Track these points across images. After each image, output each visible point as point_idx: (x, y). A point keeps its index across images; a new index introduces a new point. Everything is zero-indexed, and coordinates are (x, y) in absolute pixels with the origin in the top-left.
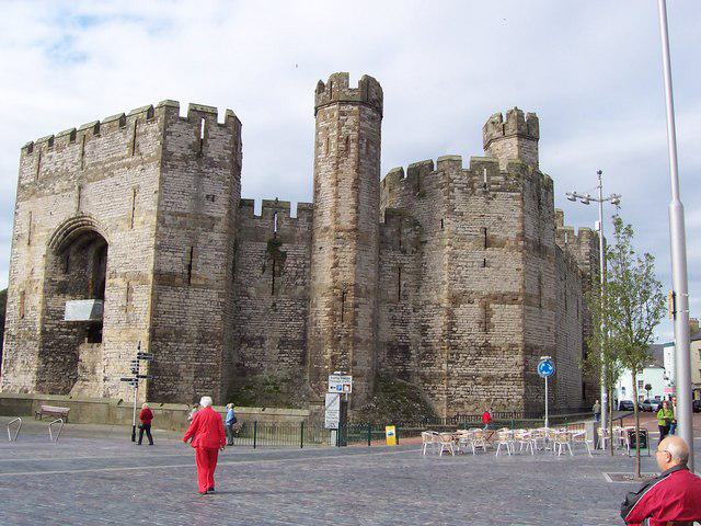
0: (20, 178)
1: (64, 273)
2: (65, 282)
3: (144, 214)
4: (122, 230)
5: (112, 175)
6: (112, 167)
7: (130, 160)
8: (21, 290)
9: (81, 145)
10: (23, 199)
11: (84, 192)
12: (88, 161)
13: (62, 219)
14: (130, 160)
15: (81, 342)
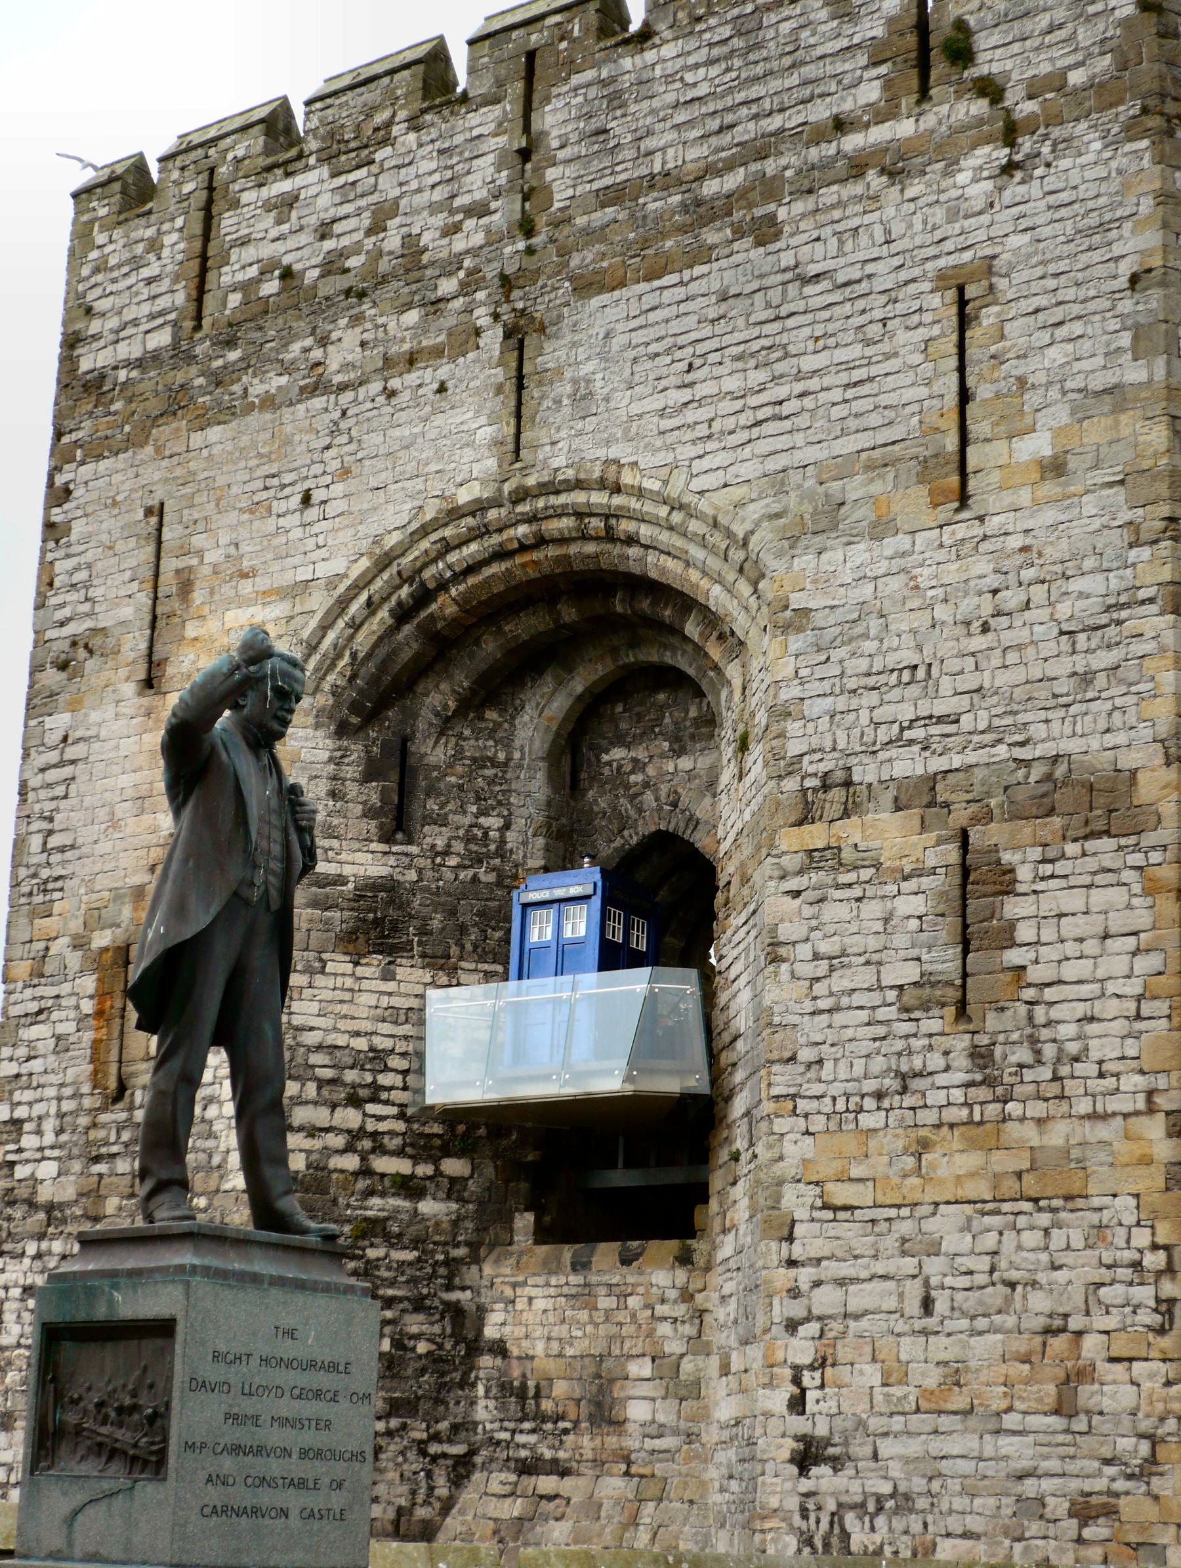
0: (72, 342)
1: (387, 838)
2: (389, 886)
3: (1061, 415)
4: (880, 529)
5: (766, 232)
6: (770, 188)
7: (905, 128)
8: (102, 939)
9: (510, 106)
10: (96, 451)
11: (549, 355)
12: (562, 183)
13: (391, 519)
14: (905, 128)
15: (487, 1233)
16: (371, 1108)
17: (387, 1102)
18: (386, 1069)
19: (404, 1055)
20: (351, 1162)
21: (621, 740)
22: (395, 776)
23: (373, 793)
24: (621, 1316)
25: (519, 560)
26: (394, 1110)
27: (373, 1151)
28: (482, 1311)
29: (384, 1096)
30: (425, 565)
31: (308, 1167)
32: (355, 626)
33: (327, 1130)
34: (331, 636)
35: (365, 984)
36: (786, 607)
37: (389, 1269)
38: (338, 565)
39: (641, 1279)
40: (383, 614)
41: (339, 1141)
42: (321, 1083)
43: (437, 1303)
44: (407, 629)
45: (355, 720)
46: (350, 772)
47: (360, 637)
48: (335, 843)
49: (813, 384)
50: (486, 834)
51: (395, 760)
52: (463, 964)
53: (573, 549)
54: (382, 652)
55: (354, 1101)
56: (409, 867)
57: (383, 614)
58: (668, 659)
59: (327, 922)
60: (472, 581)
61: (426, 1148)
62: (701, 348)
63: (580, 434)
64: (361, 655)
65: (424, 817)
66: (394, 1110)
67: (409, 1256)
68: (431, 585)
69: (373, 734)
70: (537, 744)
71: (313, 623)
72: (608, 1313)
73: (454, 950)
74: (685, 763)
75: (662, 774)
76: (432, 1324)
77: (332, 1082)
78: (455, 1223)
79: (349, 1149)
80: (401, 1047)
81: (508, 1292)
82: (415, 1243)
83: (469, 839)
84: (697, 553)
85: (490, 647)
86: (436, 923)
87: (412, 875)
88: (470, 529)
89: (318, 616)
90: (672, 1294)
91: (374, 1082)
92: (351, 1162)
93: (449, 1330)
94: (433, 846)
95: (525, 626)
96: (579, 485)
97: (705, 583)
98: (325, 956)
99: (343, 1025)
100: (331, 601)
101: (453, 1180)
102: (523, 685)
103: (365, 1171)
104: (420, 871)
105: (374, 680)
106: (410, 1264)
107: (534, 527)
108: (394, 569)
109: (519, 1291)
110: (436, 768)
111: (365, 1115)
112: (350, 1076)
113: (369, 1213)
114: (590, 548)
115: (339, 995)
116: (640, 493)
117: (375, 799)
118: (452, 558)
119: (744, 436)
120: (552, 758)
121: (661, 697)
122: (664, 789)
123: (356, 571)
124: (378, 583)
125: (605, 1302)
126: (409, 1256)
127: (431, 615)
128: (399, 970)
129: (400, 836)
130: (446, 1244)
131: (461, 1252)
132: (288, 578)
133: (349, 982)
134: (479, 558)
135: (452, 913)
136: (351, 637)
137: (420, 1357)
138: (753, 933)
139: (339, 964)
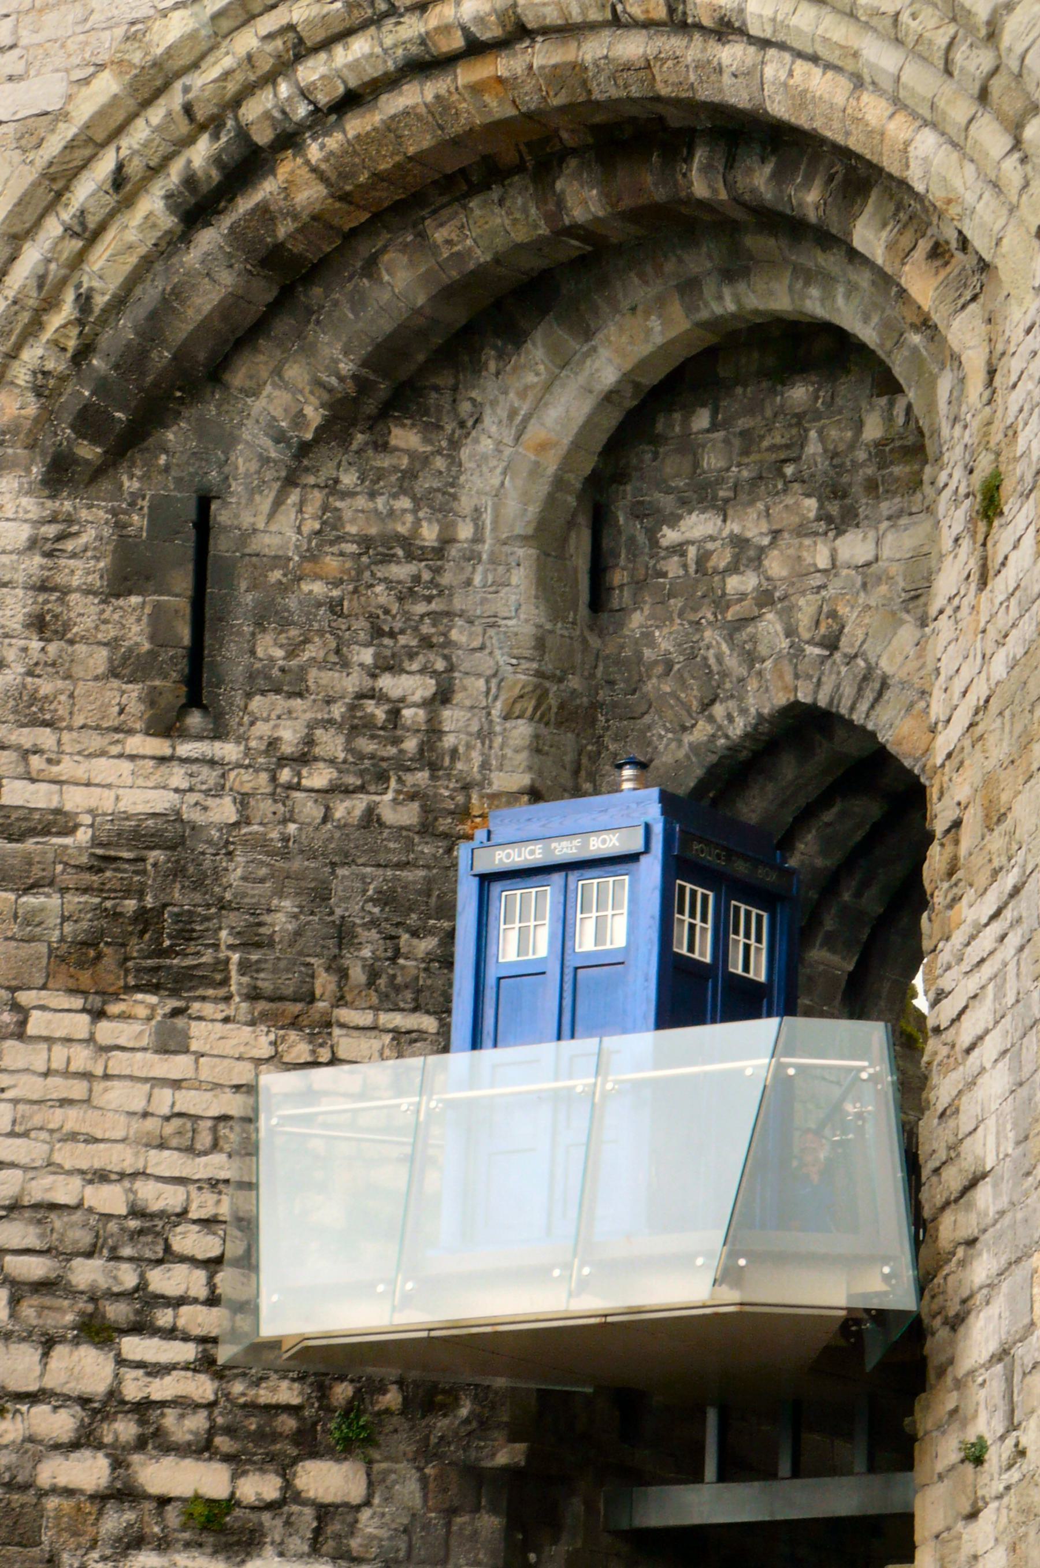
1: (166, 725)
16: (133, 1347)
17: (171, 1333)
18: (169, 1256)
19: (209, 1223)
20: (89, 1471)
21: (704, 495)
22: (183, 581)
23: (132, 622)
25: (466, 74)
26: (188, 1352)
27: (140, 1444)
29: (164, 1318)
30: (248, 90)
32: (88, 233)
33: (33, 1398)
35: (119, 1063)
38: (44, 92)
40: (153, 204)
41: (60, 1423)
44: (209, 239)
45: (89, 452)
46: (80, 571)
47: (99, 257)
48: (46, 738)
50: (395, 714)
51: (185, 543)
52: (345, 1014)
53: (592, 50)
54: (150, 293)
55: (95, 1331)
56: (217, 791)
58: (815, 304)
59: (30, 919)
60: (357, 124)
61: (261, 1436)
64: (100, 301)
65: (252, 676)
66: (188, 1352)
69: (130, 485)
70: (512, 506)
73: (324, 983)
74: (855, 547)
75: (801, 572)
77: (44, 1286)
79: (83, 1440)
80: (203, 1205)
83: (356, 726)
84: (880, 56)
85: (400, 283)
86: (281, 920)
87: (225, 810)
91: (142, 1286)
92: (89, 1471)
94: (273, 743)
95: (485, 231)
97: (898, 128)
98: (25, 998)
99: (69, 1156)
100: (30, 175)
101: (324, 1512)
102: (477, 368)
103: (123, 1493)
104: (243, 800)
105: (133, 360)
108: (175, 99)
110: (279, 561)
111: (121, 1362)
112: (86, 1273)
114: (632, 47)
115: (59, 1088)
117: (137, 635)
118: (311, 71)
120: (547, 537)
121: (799, 394)
122: (806, 608)
123: (84, 109)
124: (139, 134)
127: (264, 213)
128: (197, 1029)
129: (195, 720)
133: (81, 1058)
134: (373, 71)
135: (320, 896)
136: (79, 259)
138: (1014, 940)
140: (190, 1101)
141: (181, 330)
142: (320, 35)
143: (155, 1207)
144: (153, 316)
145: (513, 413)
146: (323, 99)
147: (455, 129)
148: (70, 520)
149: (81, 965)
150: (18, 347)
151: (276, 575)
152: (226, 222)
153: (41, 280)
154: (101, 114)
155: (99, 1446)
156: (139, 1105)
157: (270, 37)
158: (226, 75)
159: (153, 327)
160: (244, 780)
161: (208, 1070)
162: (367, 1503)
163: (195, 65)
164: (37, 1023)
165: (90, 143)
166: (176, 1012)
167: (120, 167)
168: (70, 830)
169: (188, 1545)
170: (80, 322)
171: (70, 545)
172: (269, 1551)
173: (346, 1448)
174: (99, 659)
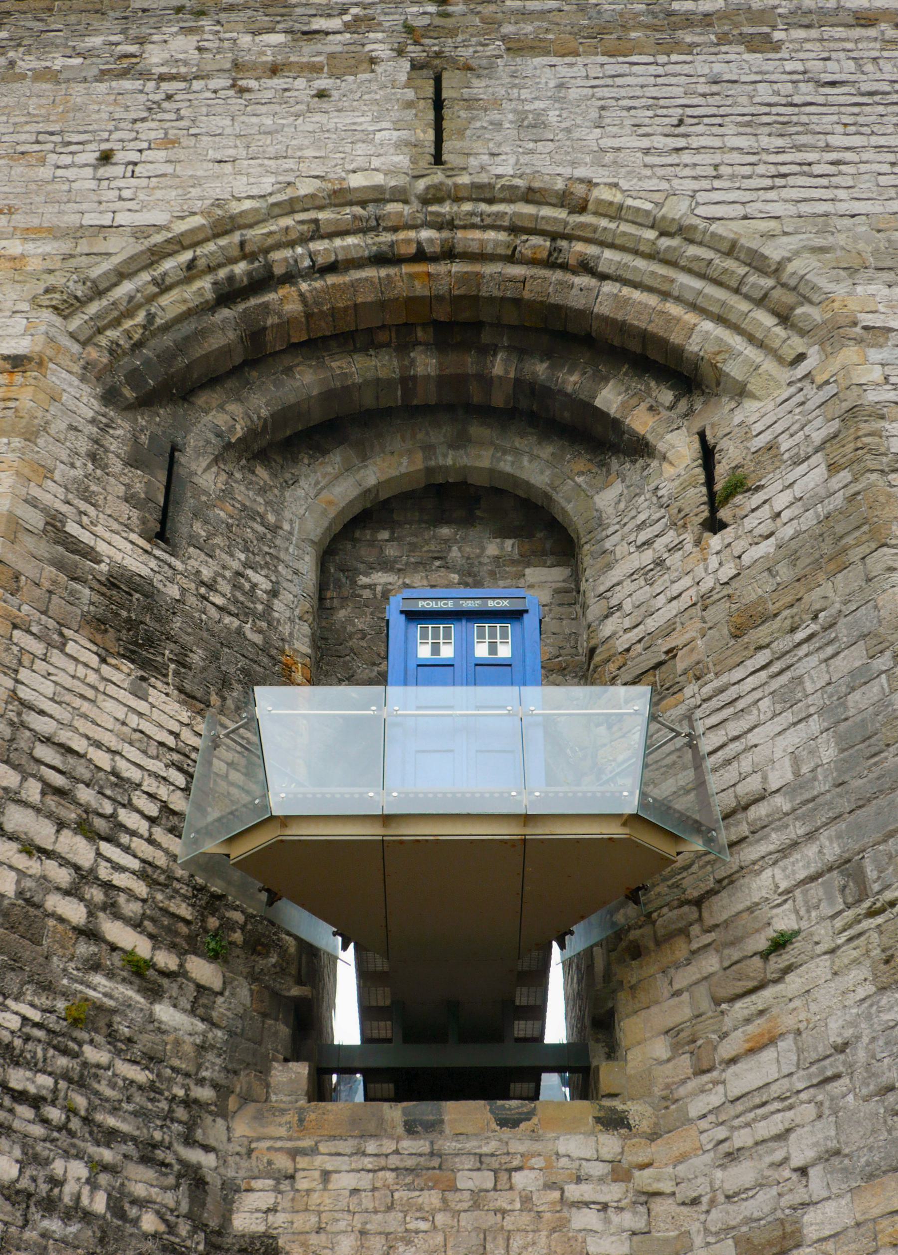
13: (247, 185)
16: (106, 848)
17: (127, 849)
18: (129, 805)
21: (386, 566)
23: (138, 481)
24: (502, 1201)
27: (104, 908)
28: (231, 1190)
29: (125, 839)
30: (278, 246)
31: (20, 894)
32: (163, 286)
34: (126, 288)
36: (855, 324)
37: (113, 1085)
39: (537, 1147)
40: (205, 284)
42: (49, 789)
43: (170, 1158)
45: (128, 393)
47: (165, 300)
48: (91, 510)
49: (849, 156)
54: (188, 328)
57: (205, 284)
60: (332, 279)
61: (169, 930)
62: (689, 111)
63: (532, 152)
64: (159, 321)
65: (191, 537)
67: (141, 1076)
68: (278, 270)
69: (142, 422)
70: (310, 525)
71: (106, 266)
72: (477, 1199)
76: (165, 1189)
77: (60, 792)
78: (202, 1048)
80: (150, 785)
81: (283, 1162)
82: (151, 1060)
85: (306, 381)
86: (197, 658)
88: (355, 217)
89: (116, 260)
90: (598, 1169)
91: (114, 815)
93: (184, 1207)
96: (531, 195)
98: (66, 632)
102: (295, 460)
103: (90, 934)
104: (183, 591)
105: (168, 357)
106: (140, 1088)
107: (445, 234)
108: (236, 237)
109: (302, 1162)
111: (99, 854)
113: (91, 993)
116: (617, 212)
118: (318, 246)
119: (768, 182)
121: (445, 531)
123: (181, 227)
124: (211, 247)
125: (467, 1180)
126: (141, 1076)
130: (187, 1075)
131: (205, 1094)
132: (72, 219)
133: (92, 678)
134: (354, 254)
135: (215, 657)
137: (146, 1236)
139: (81, 647)
140: (145, 726)
141: (198, 352)
142: (332, 229)
143: (125, 775)
144: (187, 339)
145: (317, 483)
146: (320, 260)
147: (387, 296)
148: (112, 420)
149: (98, 630)
150: (105, 328)
151: (204, 498)
152: (241, 307)
153: (131, 299)
154: (192, 231)
155: (82, 899)
156: (121, 716)
157: (302, 222)
158: (271, 233)
159: (182, 346)
160: (185, 583)
161: (156, 715)
162: (221, 994)
163: (251, 226)
164: (71, 648)
165: (179, 243)
166: (143, 679)
167: (194, 259)
168: (98, 562)
169: (124, 980)
170: (144, 327)
171: (111, 431)
172: (166, 1001)
173: (214, 956)
174: (121, 490)
